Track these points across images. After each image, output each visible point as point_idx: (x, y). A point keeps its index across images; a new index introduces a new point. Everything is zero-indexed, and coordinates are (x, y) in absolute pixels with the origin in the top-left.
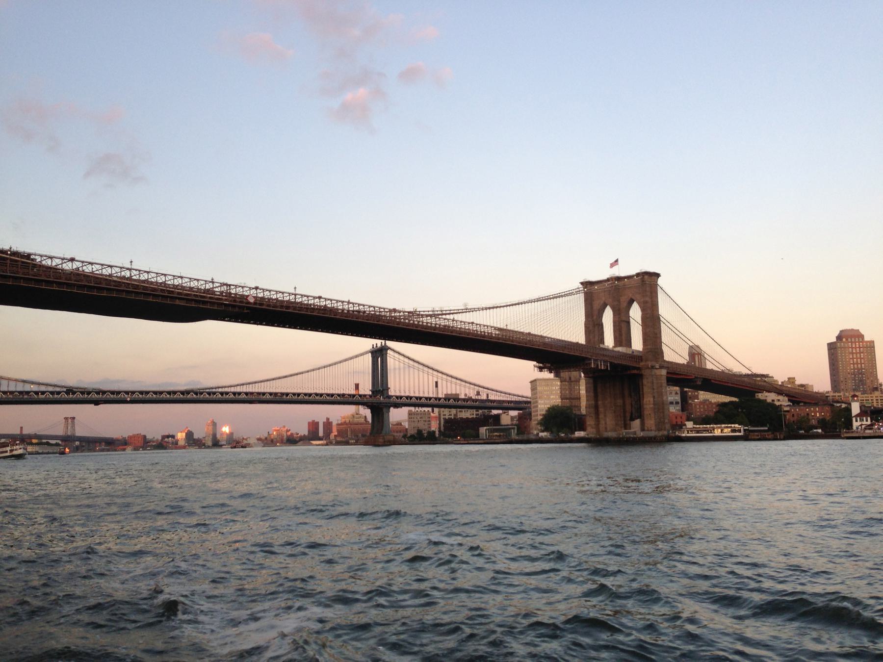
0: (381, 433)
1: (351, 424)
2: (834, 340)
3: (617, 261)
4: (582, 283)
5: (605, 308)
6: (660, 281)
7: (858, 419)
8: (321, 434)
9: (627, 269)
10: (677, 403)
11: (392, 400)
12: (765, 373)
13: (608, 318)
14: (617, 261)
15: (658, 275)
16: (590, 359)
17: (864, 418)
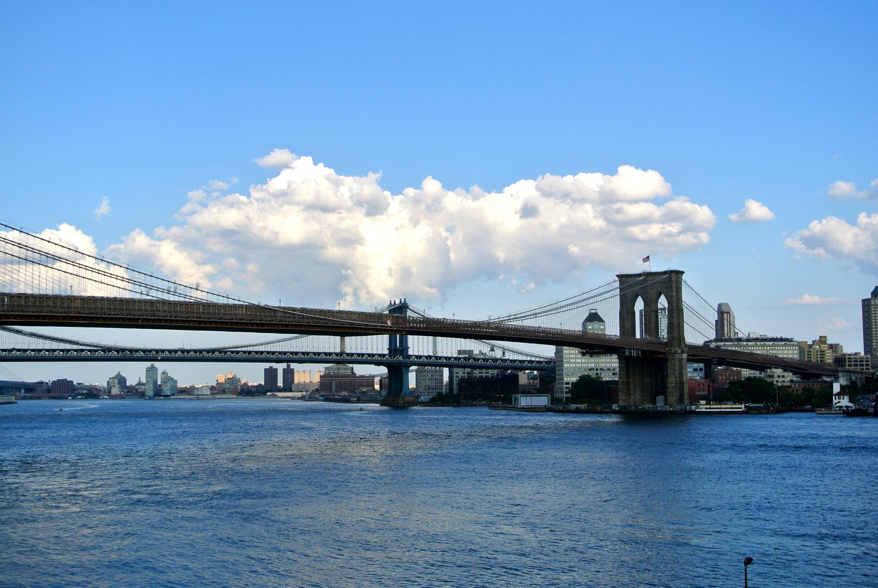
0: (400, 394)
1: (336, 377)
2: (869, 296)
3: (648, 257)
4: (617, 276)
5: (638, 296)
6: (684, 277)
7: (837, 397)
8: (280, 384)
9: (656, 266)
10: (701, 370)
11: (411, 359)
12: (789, 337)
13: (639, 305)
14: (648, 257)
15: (682, 273)
16: (625, 349)
17: (842, 397)
